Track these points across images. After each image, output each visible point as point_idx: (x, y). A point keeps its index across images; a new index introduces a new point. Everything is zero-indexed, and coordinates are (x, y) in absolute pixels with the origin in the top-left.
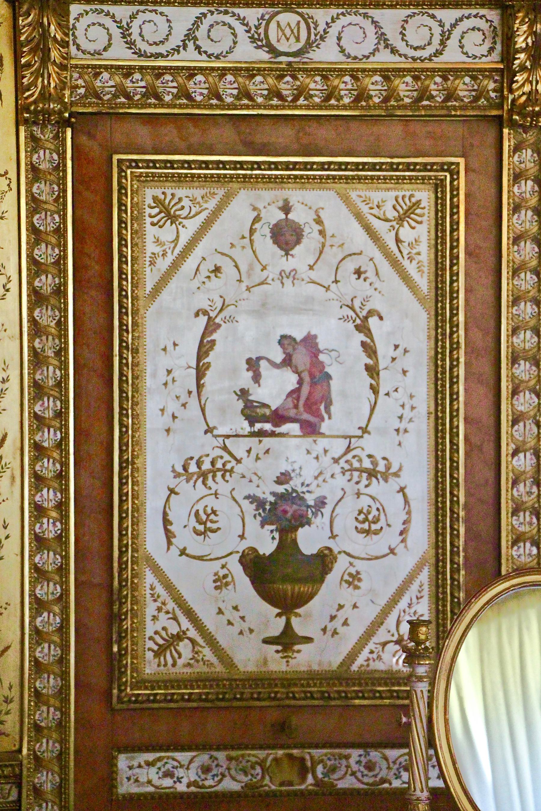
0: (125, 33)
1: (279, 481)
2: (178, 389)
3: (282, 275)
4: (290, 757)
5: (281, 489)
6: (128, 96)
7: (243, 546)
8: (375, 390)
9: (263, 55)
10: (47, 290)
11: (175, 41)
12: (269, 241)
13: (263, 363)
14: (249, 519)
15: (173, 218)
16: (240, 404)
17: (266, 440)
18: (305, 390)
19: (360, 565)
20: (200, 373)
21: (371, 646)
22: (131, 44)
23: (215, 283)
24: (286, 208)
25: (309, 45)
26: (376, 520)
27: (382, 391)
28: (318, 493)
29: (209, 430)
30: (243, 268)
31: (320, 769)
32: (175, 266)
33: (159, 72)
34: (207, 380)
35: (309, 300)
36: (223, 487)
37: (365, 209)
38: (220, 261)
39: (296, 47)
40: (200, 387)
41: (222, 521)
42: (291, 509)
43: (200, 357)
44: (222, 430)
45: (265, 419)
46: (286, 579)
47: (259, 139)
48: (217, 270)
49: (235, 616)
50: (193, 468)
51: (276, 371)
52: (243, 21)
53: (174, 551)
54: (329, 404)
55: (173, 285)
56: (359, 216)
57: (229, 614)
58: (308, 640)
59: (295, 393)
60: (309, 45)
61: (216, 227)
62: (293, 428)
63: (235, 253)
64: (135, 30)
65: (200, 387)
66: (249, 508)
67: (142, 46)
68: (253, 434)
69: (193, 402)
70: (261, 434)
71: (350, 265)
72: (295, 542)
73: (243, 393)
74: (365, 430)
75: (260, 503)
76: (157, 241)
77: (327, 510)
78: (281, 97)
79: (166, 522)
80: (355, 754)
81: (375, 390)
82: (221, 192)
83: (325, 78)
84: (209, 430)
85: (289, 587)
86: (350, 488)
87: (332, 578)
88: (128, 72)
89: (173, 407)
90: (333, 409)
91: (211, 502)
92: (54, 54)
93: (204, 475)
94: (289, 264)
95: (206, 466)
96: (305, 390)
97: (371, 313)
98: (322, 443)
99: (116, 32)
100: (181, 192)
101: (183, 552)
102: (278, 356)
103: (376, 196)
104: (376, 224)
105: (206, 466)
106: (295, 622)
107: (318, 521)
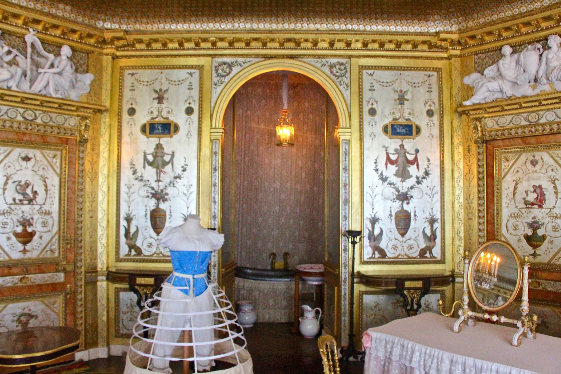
0: (497, 123)
1: (533, 219)
2: (509, 198)
3: (533, 172)
4: (536, 282)
5: (533, 220)
6: (498, 136)
7: (524, 233)
8: (557, 198)
9: (528, 123)
10: (481, 177)
11: (508, 123)
12: (530, 164)
13: (529, 192)
14: (526, 227)
15: (508, 160)
16: (523, 201)
17: (530, 210)
18: (539, 197)
19: (553, 239)
20: (514, 194)
21: (556, 258)
22: (498, 125)
23: (518, 174)
24: (534, 157)
25: (538, 120)
26: (557, 228)
27: (559, 198)
28: (542, 221)
29: (516, 207)
30: (524, 170)
31: (543, 285)
32: (509, 171)
33: (504, 130)
34: (516, 195)
35: (540, 177)
36: (519, 220)
37: (554, 155)
38: (519, 169)
39: (535, 120)
40: (514, 197)
41: (519, 228)
42: (536, 225)
43: (514, 191)
44: (519, 207)
45: (529, 204)
46: (534, 241)
47: (527, 142)
48: (518, 171)
49: (523, 249)
50: (513, 215)
51: (532, 194)
52: (523, 117)
53: (509, 234)
54: (545, 201)
55: (508, 175)
56: (552, 157)
57: (521, 248)
58: (540, 255)
59: (537, 198)
60: (538, 120)
61: (518, 162)
62: (536, 206)
63: (522, 167)
64: (499, 122)
65: (514, 197)
66: (526, 225)
67: (501, 125)
68: (526, 208)
69: (513, 201)
70: (528, 208)
71: (550, 168)
72: (537, 233)
73: (524, 199)
74: (554, 207)
75: (528, 224)
76: (505, 166)
77: (545, 226)
78: (532, 132)
79: (507, 227)
80: (552, 283)
81: (557, 198)
82: (518, 154)
83: (542, 126)
84: (516, 207)
85: (535, 243)
86: (550, 221)
87: (546, 241)
88: (498, 131)
89: (508, 202)
90: (546, 202)
91: (517, 223)
92: (479, 129)
93: (515, 217)
94: (535, 169)
95: (516, 215)
96: (539, 197)
97: (556, 179)
98: (543, 210)
99: (495, 123)
100: (510, 155)
101: (511, 234)
102: (532, 190)
103: (556, 152)
104: (557, 158)
105: (516, 215)
106: (537, 251)
107: (542, 228)
